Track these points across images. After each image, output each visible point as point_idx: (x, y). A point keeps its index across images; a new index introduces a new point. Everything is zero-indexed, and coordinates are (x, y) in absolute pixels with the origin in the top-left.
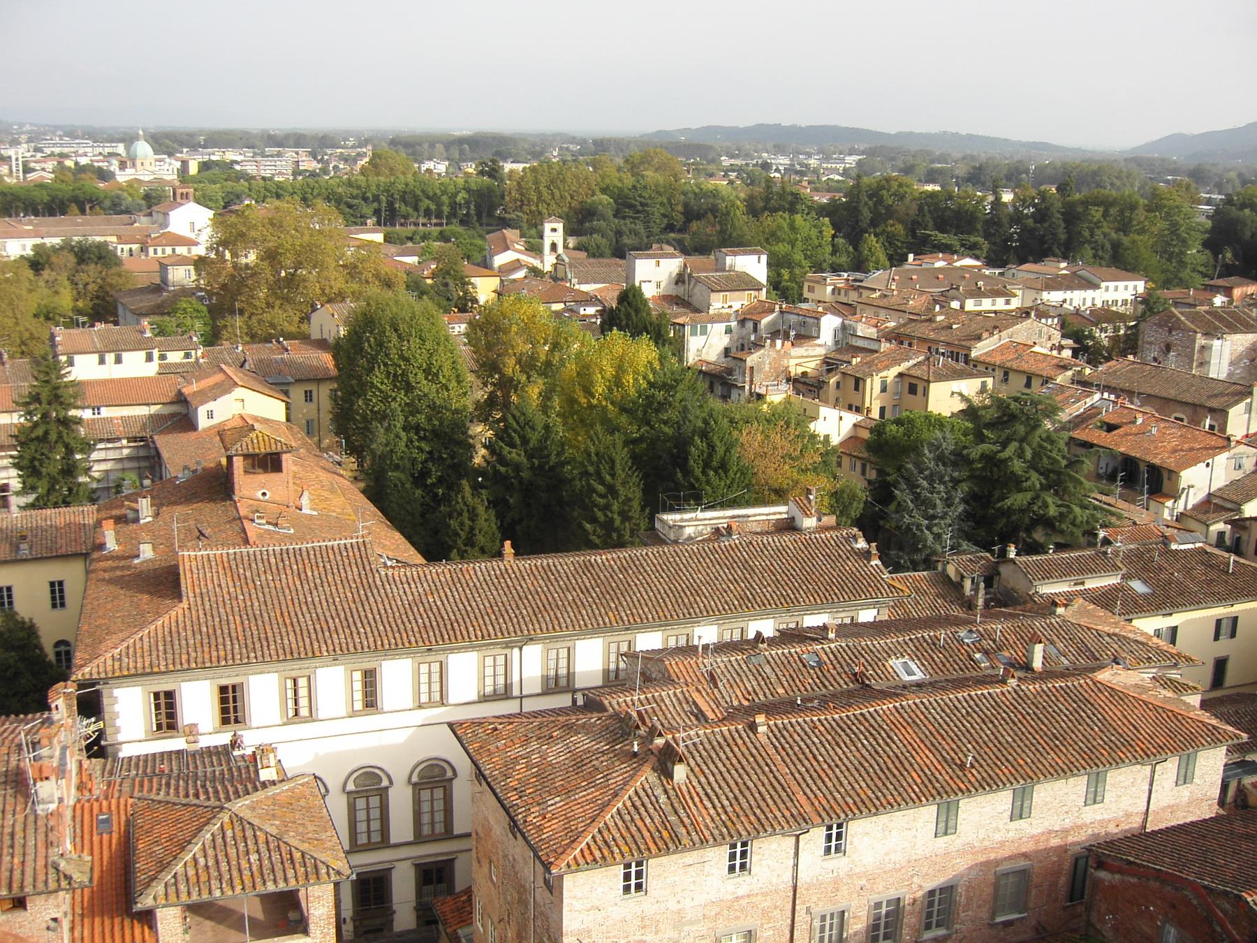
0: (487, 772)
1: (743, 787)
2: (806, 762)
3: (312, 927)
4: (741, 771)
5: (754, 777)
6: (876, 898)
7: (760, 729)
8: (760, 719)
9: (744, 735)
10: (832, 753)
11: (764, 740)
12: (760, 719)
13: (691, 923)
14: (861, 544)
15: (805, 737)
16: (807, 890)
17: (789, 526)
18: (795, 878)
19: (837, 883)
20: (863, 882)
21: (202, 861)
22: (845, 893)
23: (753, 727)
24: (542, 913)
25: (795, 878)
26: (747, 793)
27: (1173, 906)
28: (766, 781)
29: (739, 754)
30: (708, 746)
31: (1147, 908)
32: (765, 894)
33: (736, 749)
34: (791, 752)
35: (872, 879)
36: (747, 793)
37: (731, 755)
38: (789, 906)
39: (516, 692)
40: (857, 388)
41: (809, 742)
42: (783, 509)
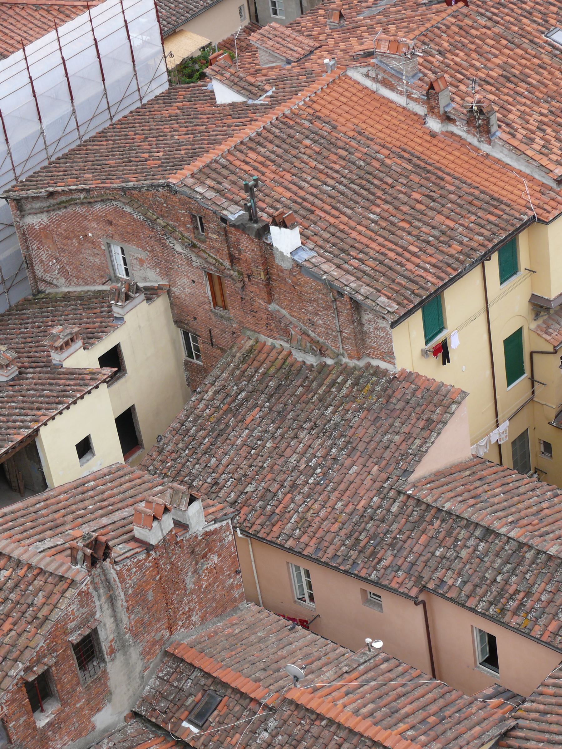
27: (110, 223)
31: (86, 236)
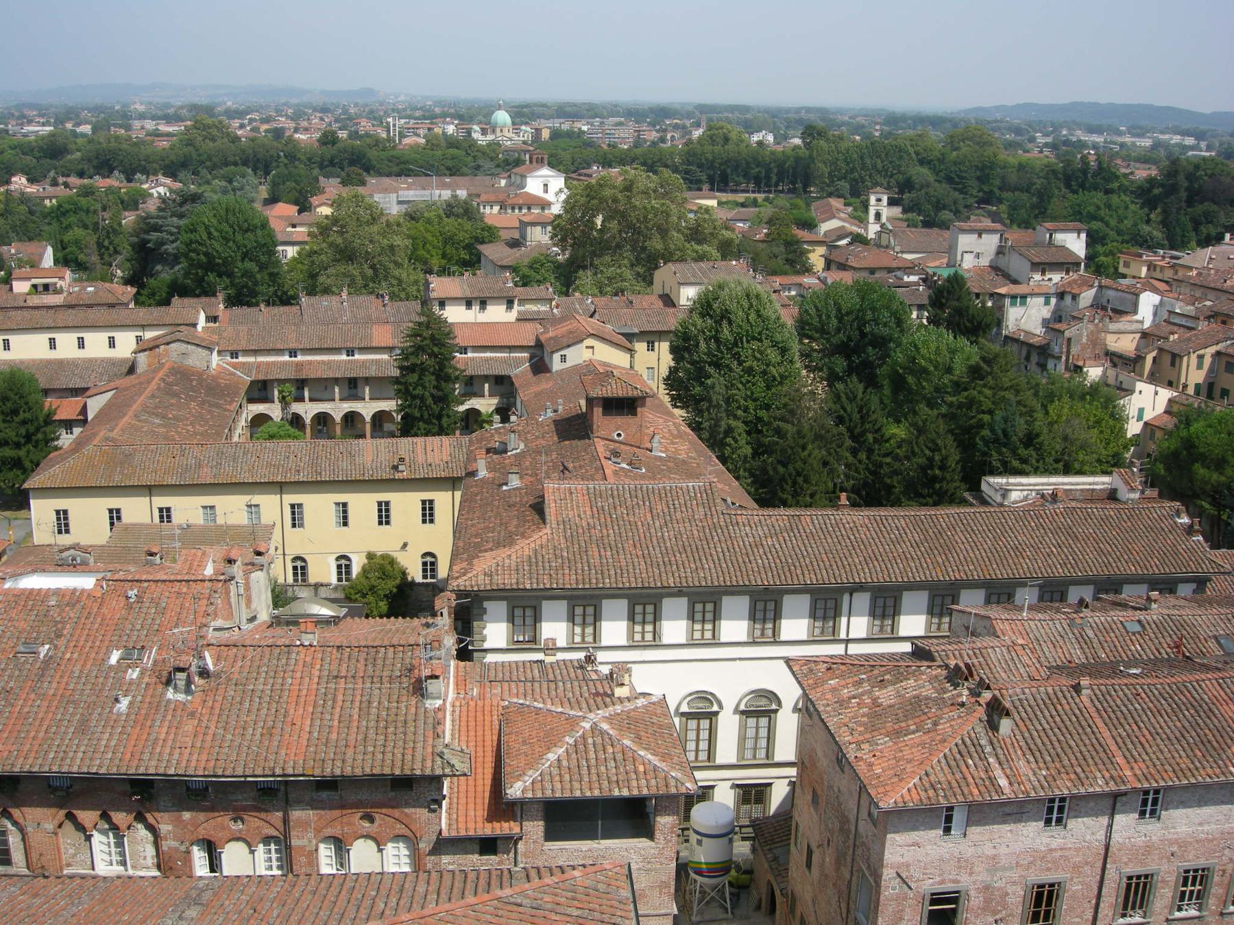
0: (821, 709)
1: (1065, 745)
2: (1127, 727)
3: (658, 834)
4: (1064, 730)
5: (1076, 737)
6: (1187, 865)
7: (1084, 692)
8: (1085, 682)
9: (1068, 695)
10: (1153, 720)
11: (1088, 704)
12: (1085, 682)
13: (1004, 869)
14: (1185, 520)
15: (1127, 702)
16: (1119, 850)
17: (1112, 495)
18: (1109, 837)
19: (1148, 849)
20: (1175, 849)
21: (565, 763)
22: (1156, 858)
23: (1077, 688)
24: (863, 844)
25: (1109, 837)
26: (1069, 751)
28: (1087, 742)
29: (1062, 712)
30: (1032, 703)
32: (1078, 850)
33: (1059, 707)
34: (1113, 716)
35: (1183, 844)
36: (1069, 751)
37: (1054, 713)
38: (1099, 864)
39: (843, 635)
40: (1173, 364)
41: (1130, 707)
42: (1106, 479)
